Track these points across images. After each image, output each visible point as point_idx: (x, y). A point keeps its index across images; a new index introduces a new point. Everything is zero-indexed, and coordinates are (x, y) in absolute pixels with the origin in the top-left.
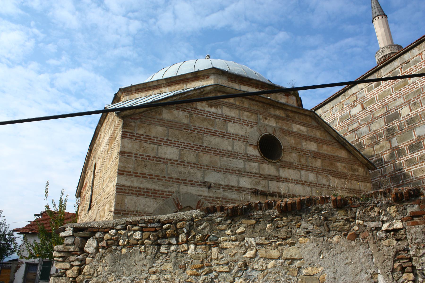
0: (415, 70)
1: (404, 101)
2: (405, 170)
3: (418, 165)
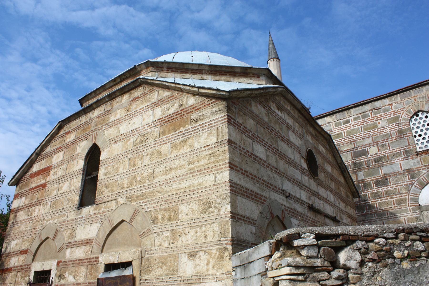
0: (384, 117)
2: (370, 201)
3: (384, 199)
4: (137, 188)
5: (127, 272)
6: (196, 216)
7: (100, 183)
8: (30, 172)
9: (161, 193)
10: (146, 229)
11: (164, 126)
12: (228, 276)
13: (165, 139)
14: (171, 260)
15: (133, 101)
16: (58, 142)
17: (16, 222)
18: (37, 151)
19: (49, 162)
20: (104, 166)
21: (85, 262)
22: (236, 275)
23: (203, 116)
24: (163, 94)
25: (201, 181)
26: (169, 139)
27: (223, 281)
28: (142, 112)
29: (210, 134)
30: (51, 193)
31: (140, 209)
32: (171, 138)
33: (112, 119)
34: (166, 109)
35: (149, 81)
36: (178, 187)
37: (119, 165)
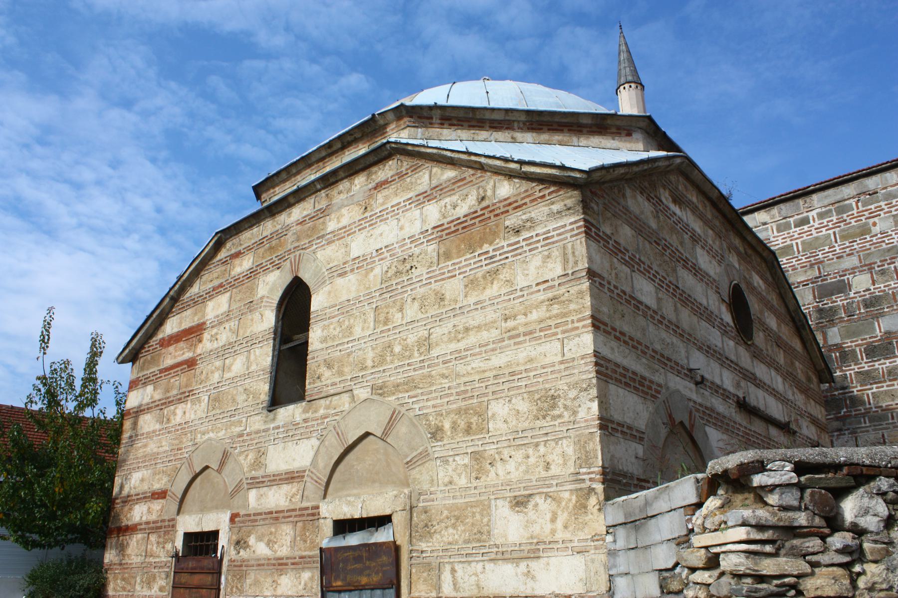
0: (887, 210)
1: (861, 262)
2: (855, 390)
3: (884, 384)
4: (396, 368)
5: (382, 536)
6: (526, 425)
7: (314, 358)
8: (160, 336)
9: (447, 377)
10: (419, 451)
11: (447, 242)
12: (596, 543)
13: (450, 268)
14: (474, 513)
15: (375, 188)
16: (215, 275)
17: (137, 435)
18: (172, 293)
19: (199, 315)
20: (321, 324)
21: (290, 516)
22: (615, 541)
23: (530, 220)
24: (442, 174)
25: (533, 354)
26: (459, 268)
27: (586, 554)
28: (396, 212)
29: (549, 257)
30: (207, 378)
31: (403, 410)
32: (463, 267)
33: (332, 225)
34: (449, 207)
35: (410, 148)
36: (483, 365)
37: (352, 321)
